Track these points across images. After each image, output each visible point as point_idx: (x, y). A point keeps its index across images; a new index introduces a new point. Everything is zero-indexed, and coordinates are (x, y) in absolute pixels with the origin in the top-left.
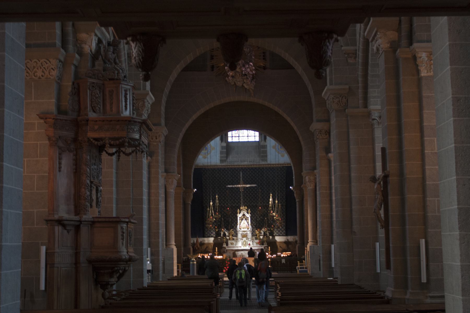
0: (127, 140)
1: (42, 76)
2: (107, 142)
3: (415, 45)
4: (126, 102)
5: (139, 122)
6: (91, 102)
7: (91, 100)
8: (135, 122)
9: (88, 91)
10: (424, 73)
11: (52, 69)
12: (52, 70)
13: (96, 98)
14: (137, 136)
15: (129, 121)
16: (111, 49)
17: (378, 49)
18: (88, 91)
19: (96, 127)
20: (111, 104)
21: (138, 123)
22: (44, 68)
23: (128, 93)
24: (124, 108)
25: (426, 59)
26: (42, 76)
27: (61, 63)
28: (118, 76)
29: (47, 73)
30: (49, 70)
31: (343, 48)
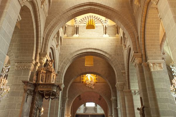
0: (52, 92)
2: (45, 92)
3: (148, 61)
4: (53, 79)
5: (57, 86)
6: (41, 78)
8: (55, 85)
10: (152, 70)
13: (43, 77)
14: (55, 91)
15: (53, 85)
16: (51, 62)
17: (135, 65)
19: (42, 87)
20: (48, 79)
24: (52, 81)
25: (152, 66)
31: (121, 71)
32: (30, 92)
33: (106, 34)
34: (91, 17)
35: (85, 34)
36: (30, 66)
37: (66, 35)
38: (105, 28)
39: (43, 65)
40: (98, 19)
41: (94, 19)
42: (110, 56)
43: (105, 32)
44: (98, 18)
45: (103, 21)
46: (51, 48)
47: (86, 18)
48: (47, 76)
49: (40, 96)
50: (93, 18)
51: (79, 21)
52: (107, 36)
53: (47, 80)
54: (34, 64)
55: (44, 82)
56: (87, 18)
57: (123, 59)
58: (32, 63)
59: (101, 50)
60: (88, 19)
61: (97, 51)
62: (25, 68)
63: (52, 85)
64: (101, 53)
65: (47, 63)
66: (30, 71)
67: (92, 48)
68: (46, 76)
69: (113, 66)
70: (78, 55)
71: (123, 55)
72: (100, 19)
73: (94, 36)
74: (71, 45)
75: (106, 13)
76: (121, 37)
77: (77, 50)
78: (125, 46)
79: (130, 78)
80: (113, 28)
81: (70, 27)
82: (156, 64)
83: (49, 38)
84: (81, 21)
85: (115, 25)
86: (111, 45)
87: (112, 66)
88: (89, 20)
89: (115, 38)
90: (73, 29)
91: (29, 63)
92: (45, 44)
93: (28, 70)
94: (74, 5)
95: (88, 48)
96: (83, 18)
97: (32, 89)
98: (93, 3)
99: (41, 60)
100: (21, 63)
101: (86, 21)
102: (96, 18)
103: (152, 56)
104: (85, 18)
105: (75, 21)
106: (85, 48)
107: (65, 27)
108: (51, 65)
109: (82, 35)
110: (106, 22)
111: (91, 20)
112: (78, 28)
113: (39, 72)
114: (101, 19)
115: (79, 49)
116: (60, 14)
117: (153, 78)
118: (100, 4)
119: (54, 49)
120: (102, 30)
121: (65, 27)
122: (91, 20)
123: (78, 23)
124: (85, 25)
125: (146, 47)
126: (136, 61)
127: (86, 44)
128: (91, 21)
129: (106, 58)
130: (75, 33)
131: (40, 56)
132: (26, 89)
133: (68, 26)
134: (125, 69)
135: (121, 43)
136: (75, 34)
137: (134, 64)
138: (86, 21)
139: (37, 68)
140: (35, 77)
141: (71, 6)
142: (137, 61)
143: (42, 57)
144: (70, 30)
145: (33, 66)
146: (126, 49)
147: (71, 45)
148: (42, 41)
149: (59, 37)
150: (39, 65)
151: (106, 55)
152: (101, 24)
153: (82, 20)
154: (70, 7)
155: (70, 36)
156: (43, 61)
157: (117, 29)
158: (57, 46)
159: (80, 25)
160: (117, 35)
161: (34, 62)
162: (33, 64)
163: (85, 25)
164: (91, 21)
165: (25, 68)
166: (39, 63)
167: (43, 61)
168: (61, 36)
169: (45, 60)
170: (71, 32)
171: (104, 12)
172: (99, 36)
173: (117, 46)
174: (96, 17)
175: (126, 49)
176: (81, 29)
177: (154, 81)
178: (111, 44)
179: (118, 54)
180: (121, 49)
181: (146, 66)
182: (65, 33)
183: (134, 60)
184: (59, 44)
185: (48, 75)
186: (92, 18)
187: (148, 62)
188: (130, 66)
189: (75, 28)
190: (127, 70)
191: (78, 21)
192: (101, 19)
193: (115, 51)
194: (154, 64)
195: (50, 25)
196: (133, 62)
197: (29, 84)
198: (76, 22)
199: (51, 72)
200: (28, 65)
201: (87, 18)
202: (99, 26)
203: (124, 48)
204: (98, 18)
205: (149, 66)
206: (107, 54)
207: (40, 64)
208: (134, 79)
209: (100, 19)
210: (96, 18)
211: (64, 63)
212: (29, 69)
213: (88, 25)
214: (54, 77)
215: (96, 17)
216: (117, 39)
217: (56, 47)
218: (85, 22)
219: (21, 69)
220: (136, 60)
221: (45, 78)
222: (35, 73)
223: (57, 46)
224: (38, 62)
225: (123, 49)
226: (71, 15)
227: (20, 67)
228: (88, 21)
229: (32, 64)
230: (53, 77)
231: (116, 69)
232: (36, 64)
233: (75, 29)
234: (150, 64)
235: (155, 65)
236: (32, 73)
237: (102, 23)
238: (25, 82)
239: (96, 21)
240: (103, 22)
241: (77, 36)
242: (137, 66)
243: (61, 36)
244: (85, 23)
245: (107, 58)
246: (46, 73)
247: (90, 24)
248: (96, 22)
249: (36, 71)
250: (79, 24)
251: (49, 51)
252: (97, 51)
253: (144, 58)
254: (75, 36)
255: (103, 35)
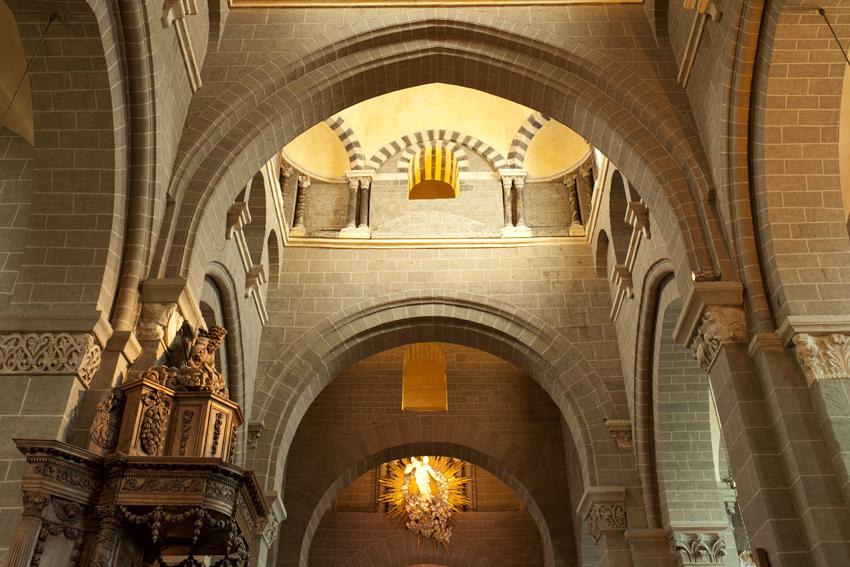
1: (53, 365)
4: (216, 438)
5: (235, 476)
6: (143, 428)
7: (143, 424)
8: (227, 473)
9: (141, 405)
10: (819, 374)
11: (76, 351)
12: (74, 355)
15: (213, 470)
16: (206, 341)
17: (706, 353)
18: (141, 405)
20: (184, 439)
21: (231, 479)
22: (61, 349)
23: (223, 420)
25: (816, 348)
26: (53, 365)
27: (97, 347)
28: (208, 383)
29: (63, 360)
30: (70, 356)
32: (66, 513)
33: (515, 223)
34: (436, 136)
35: (405, 222)
36: (75, 353)
37: (300, 230)
38: (508, 193)
39: (160, 352)
40: (474, 149)
41: (451, 145)
42: (544, 337)
43: (509, 214)
44: (471, 144)
45: (499, 157)
46: (212, 279)
47: (408, 144)
48: (180, 421)
49: (125, 549)
50: (445, 144)
51: (374, 159)
52: (522, 231)
53: (177, 440)
54: (104, 342)
55: (157, 452)
56: (414, 140)
57: (616, 353)
58: (91, 332)
59: (491, 310)
60: (418, 151)
61: (469, 311)
62: (46, 361)
63: (207, 468)
64: (494, 322)
65: (185, 345)
66: (76, 386)
67: (444, 295)
68: (173, 419)
69: (558, 397)
70: (364, 338)
71: (613, 335)
72: (481, 149)
73: (452, 235)
74: (329, 280)
75: (524, 73)
76: (603, 233)
77: (360, 309)
78: (627, 276)
79: (663, 458)
80: (555, 196)
81: (323, 189)
82: (836, 338)
83: (205, 204)
84: (383, 158)
85: (560, 181)
86: (542, 279)
87: (554, 396)
88: (423, 153)
89: (563, 242)
90: (340, 200)
91: (71, 333)
92: (180, 239)
93: (64, 374)
94: (350, 35)
95: (420, 296)
96: (394, 144)
97: (79, 494)
98: (452, 22)
99: (151, 325)
100: (22, 333)
101: (409, 156)
102: (465, 145)
103: (808, 292)
104: (402, 145)
105: (353, 158)
106: (405, 297)
107: (300, 189)
108: (207, 357)
109: (388, 230)
110: (517, 161)
111: (434, 152)
112: (366, 194)
113: (129, 395)
114: (490, 150)
115: (374, 304)
116: (272, 80)
117: (829, 422)
118: (491, 29)
119: (232, 293)
120: (495, 203)
121: (300, 189)
122: (434, 152)
123: (367, 167)
124: (403, 176)
125: (766, 244)
126: (713, 328)
127: (411, 274)
128: (434, 159)
129: (522, 350)
130: (348, 221)
131: (142, 300)
132: (38, 494)
133: (314, 181)
134: (626, 408)
135: (602, 271)
136: (353, 224)
137: (700, 354)
138: (409, 156)
139: (121, 367)
140: (101, 424)
141: (331, 42)
142: (720, 326)
143: (157, 307)
144: (322, 205)
145: (98, 354)
146: (632, 297)
147: (329, 280)
148: (158, 216)
149: (264, 229)
150: (133, 349)
151: (522, 335)
152: (486, 175)
153: (389, 155)
154: (324, 45)
155: (321, 234)
156: (159, 329)
157: (576, 196)
158: (248, 276)
159: (377, 178)
160: (575, 229)
161: (105, 329)
162: (97, 342)
163: (403, 176)
164: (434, 159)
165: (46, 361)
166: (133, 337)
167: (159, 329)
168: (273, 232)
169: (174, 325)
170: (332, 216)
171: (512, 69)
172: (479, 234)
173: (576, 286)
174: (460, 140)
175: (632, 297)
176: (386, 200)
177: (838, 437)
178: (546, 274)
179: (584, 328)
180: (601, 300)
181: (771, 353)
182: (296, 217)
183: (700, 323)
184: (261, 270)
185: (186, 413)
186: (439, 145)
187: (790, 328)
188: (661, 389)
189: (351, 191)
190: (643, 414)
191: (368, 157)
192: (490, 150)
193: (570, 313)
194: (823, 336)
195: (211, 134)
196: (691, 341)
197: (64, 463)
198: (354, 164)
199: (204, 395)
200: (64, 345)
201: (414, 140)
202: (476, 181)
203: (616, 290)
204: (471, 144)
205: (799, 349)
206: (523, 331)
207: (139, 348)
208: (684, 465)
209: (481, 149)
210: (465, 145)
211: (290, 379)
212: (71, 370)
213: (418, 181)
214: (222, 427)
215: (460, 140)
216: (575, 248)
217: (247, 285)
218: (404, 165)
219: (22, 370)
220: (712, 322)
221: (164, 429)
222: (104, 398)
223: (251, 278)
224: (128, 334)
225: (610, 304)
226: (330, 84)
227: (17, 362)
228: (422, 161)
229: (91, 339)
230: (218, 422)
231: (577, 412)
232: (117, 343)
233: (351, 199)
234: (803, 337)
235: (834, 343)
236: (87, 399)
237: (495, 170)
238: (33, 450)
239: (463, 159)
240: (497, 164)
241: (362, 232)
242: (723, 358)
243: (273, 232)
244: (403, 170)
245: (527, 352)
246: (175, 398)
247: (428, 177)
248: (462, 164)
249: (114, 385)
250: (371, 173)
251: (197, 290)
252: (468, 315)
253: (758, 307)
254: (351, 232)
255: (502, 229)
